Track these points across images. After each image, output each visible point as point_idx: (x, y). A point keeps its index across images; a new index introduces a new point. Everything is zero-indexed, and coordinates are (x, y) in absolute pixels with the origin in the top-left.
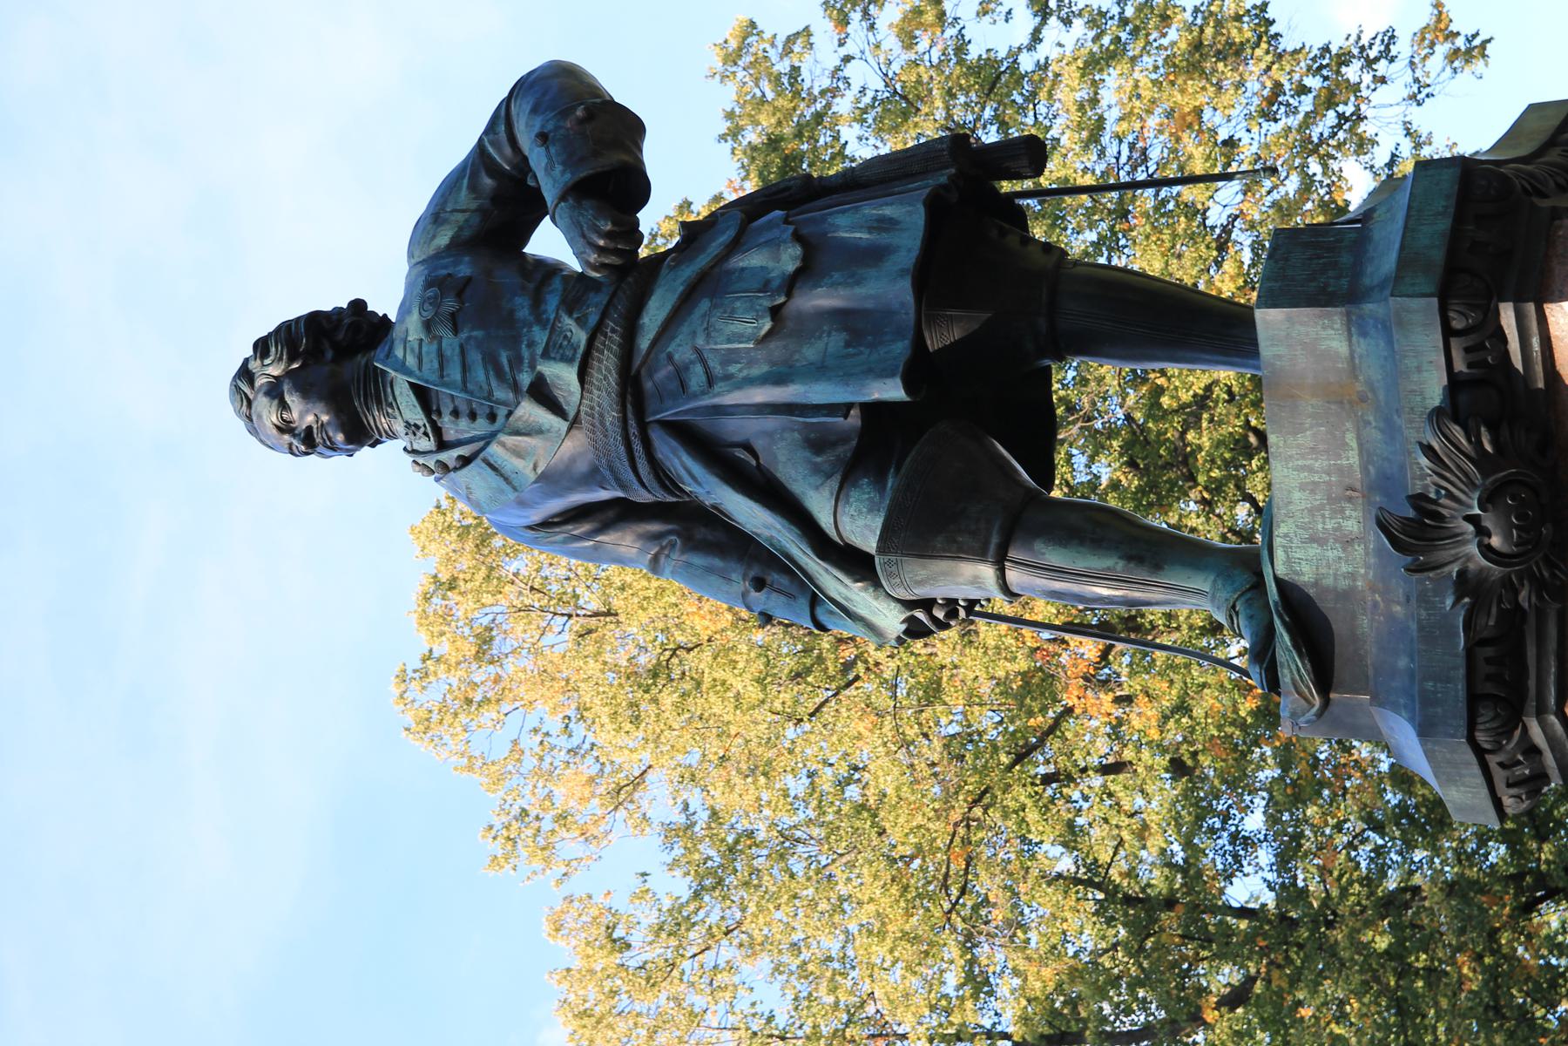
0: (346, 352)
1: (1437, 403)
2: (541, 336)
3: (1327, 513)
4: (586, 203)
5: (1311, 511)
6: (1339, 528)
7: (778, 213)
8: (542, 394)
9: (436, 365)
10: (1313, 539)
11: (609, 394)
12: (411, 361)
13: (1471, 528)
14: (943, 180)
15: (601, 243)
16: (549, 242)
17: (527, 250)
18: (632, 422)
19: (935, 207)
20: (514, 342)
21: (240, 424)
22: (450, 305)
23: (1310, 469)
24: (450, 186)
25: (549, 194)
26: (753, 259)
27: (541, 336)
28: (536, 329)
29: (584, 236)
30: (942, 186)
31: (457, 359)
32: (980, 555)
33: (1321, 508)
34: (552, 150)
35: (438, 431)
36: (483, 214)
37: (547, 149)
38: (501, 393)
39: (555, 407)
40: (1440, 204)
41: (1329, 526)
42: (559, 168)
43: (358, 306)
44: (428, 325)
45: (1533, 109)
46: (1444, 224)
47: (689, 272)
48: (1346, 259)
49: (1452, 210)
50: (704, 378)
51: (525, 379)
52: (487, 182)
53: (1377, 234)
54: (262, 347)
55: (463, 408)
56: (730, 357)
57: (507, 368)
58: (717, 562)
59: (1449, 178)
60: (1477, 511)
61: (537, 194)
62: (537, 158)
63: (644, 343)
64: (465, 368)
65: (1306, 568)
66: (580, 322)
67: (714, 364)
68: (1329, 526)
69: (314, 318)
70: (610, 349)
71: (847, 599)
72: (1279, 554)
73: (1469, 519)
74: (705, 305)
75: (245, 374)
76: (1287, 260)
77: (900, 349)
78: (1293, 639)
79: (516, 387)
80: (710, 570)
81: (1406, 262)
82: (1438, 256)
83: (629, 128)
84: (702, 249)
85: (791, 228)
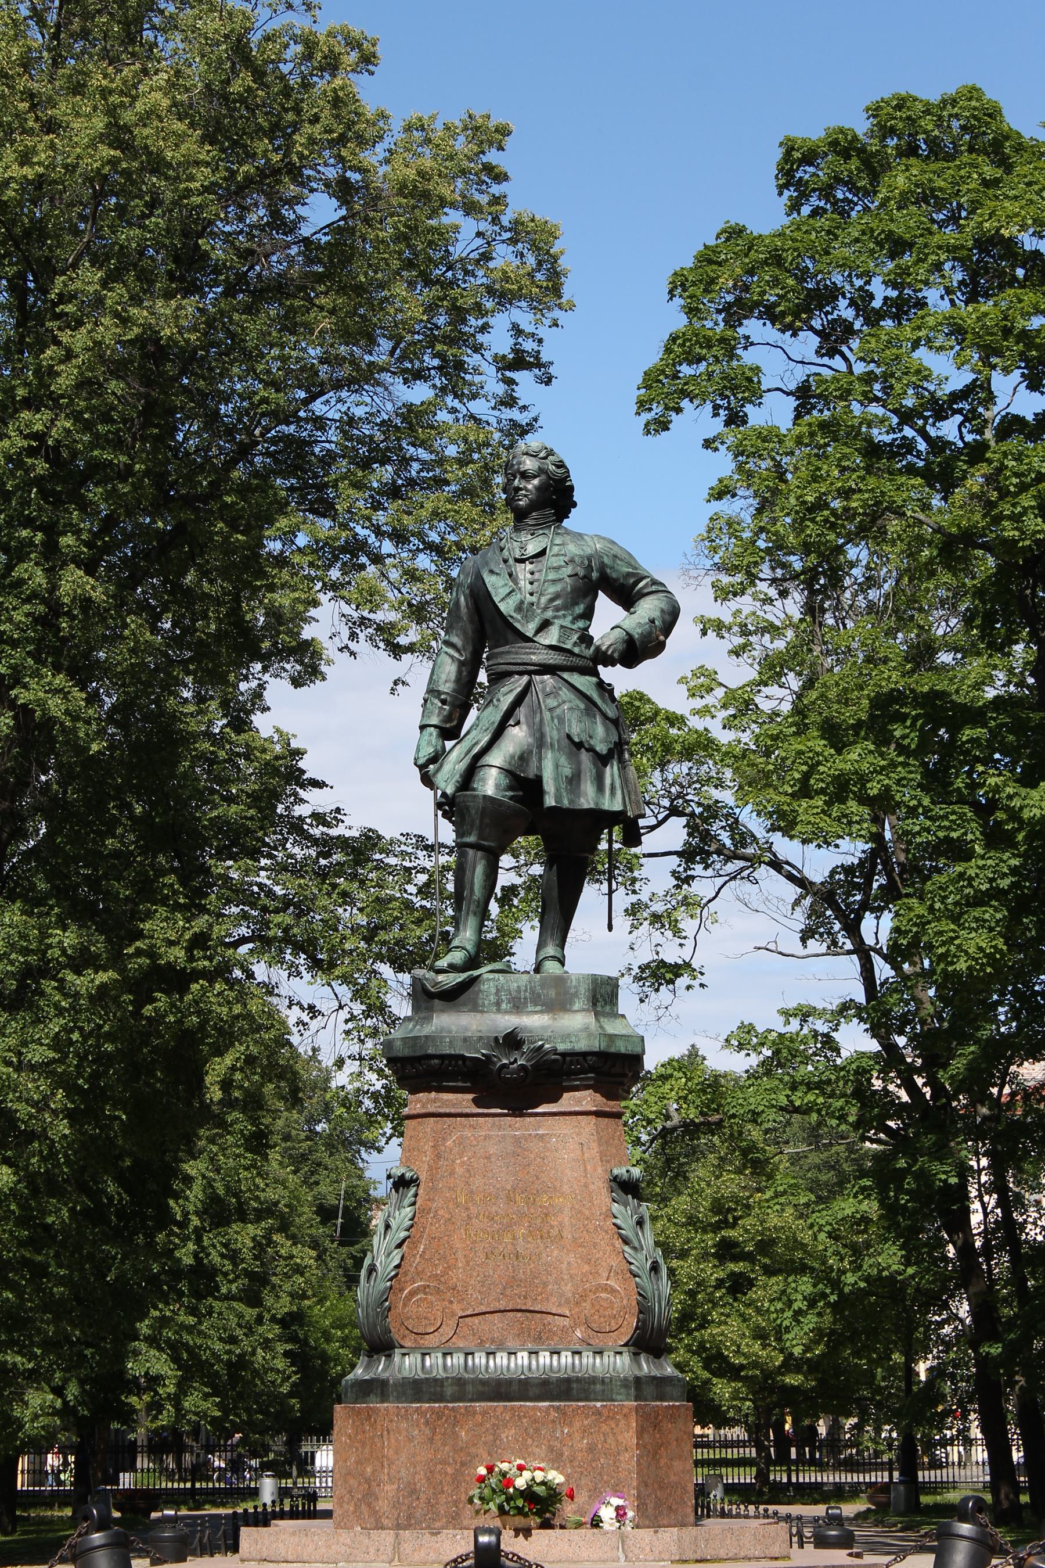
0: (553, 505)
2: (567, 622)
8: (545, 625)
12: (556, 549)
20: (565, 607)
26: (600, 730)
27: (567, 622)
32: (481, 837)
35: (521, 561)
38: (544, 600)
43: (574, 505)
44: (572, 561)
46: (623, 1050)
47: (595, 696)
48: (608, 1008)
51: (549, 614)
53: (618, 1021)
54: (561, 465)
55: (537, 576)
56: (561, 720)
63: (566, 675)
64: (554, 581)
66: (575, 644)
67: (558, 711)
69: (571, 488)
72: (491, 976)
74: (582, 706)
75: (551, 453)
77: (566, 803)
79: (545, 609)
81: (612, 1037)
82: (613, 1050)
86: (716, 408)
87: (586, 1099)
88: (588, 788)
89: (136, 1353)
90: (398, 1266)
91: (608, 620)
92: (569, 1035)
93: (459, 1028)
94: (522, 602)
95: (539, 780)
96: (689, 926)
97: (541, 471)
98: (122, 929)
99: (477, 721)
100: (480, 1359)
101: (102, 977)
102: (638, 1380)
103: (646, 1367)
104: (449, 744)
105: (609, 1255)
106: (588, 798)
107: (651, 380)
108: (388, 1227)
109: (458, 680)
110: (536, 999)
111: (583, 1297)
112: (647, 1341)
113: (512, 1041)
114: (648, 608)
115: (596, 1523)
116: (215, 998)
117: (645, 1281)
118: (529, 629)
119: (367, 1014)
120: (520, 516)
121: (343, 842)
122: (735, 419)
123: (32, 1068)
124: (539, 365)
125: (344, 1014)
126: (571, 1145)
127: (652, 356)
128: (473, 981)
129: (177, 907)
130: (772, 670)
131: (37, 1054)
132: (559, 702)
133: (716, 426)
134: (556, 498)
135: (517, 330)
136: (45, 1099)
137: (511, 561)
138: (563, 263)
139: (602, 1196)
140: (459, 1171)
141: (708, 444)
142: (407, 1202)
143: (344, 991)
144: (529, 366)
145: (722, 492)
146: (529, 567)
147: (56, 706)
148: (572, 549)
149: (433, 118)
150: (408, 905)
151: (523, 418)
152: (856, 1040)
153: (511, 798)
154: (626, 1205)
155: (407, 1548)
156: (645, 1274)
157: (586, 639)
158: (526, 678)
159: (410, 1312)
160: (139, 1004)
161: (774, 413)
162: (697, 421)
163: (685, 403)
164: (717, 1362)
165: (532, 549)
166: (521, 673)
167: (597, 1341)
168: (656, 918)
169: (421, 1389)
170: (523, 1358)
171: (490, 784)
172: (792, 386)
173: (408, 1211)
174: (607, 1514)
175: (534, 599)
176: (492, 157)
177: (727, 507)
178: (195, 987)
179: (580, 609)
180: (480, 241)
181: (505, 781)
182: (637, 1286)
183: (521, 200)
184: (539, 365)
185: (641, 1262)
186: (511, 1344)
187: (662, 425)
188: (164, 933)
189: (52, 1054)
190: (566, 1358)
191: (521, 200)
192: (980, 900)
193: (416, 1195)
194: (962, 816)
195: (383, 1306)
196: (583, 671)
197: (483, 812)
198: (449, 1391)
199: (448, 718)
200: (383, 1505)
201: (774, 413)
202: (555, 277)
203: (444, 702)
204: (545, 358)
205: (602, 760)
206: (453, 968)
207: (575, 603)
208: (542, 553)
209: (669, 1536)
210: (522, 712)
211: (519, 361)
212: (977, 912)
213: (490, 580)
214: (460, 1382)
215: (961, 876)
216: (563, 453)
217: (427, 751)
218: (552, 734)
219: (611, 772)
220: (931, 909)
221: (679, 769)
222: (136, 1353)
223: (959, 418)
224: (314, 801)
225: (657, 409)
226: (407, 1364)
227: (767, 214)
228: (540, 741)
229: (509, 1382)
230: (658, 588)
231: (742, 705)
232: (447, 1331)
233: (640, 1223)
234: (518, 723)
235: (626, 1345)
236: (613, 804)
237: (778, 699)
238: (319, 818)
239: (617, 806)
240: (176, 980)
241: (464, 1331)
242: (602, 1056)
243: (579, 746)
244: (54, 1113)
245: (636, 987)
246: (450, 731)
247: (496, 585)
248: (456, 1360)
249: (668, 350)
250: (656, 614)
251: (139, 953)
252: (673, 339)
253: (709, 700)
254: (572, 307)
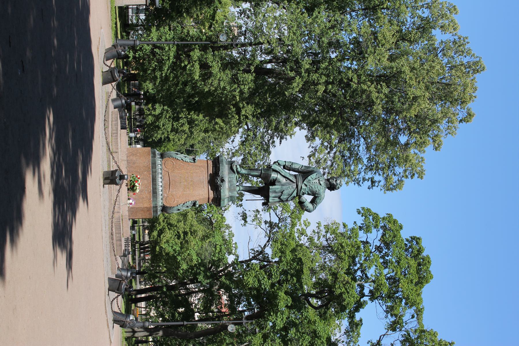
0: (331, 187)
2: (307, 190)
8: (306, 186)
24: (320, 202)
27: (307, 190)
51: (308, 186)
75: (341, 186)
77: (270, 190)
81: (224, 200)
86: (363, 224)
87: (212, 196)
88: (274, 195)
89: (160, 106)
91: (307, 198)
93: (225, 170)
95: (275, 185)
96: (255, 223)
97: (337, 184)
98: (249, 100)
99: (286, 172)
100: (160, 176)
101: (238, 98)
102: (157, 207)
103: (159, 209)
104: (282, 167)
105: (181, 201)
106: (271, 195)
107: (369, 210)
110: (231, 185)
111: (173, 196)
112: (164, 209)
113: (223, 181)
114: (310, 206)
115: (129, 199)
116: (235, 121)
117: (176, 208)
118: (305, 182)
119: (233, 153)
120: (328, 180)
121: (268, 147)
122: (361, 228)
123: (219, 83)
124: (372, 186)
125: (232, 148)
126: (203, 193)
127: (374, 210)
128: (234, 173)
129: (254, 112)
130: (311, 239)
131: (222, 84)
132: (290, 189)
133: (359, 224)
134: (332, 187)
135: (380, 182)
136: (212, 86)
138: (394, 191)
139: (193, 199)
140: (197, 171)
141: (355, 222)
143: (237, 148)
144: (372, 184)
145: (345, 226)
147: (295, 85)
148: (322, 191)
149: (424, 163)
150: (256, 161)
151: (361, 183)
152: (231, 259)
155: (123, 162)
156: (178, 208)
157: (304, 194)
159: (169, 161)
160: (233, 105)
161: (362, 236)
162: (360, 220)
163: (364, 217)
164: (161, 232)
165: (321, 182)
167: (164, 199)
168: (256, 216)
169: (154, 164)
170: (161, 184)
171: (274, 175)
172: (368, 240)
173: (189, 161)
174: (131, 201)
176: (416, 175)
177: (341, 227)
178: (237, 116)
179: (310, 192)
180: (398, 173)
181: (274, 178)
183: (407, 182)
184: (372, 186)
185: (180, 207)
186: (163, 182)
187: (359, 213)
188: (248, 110)
189: (222, 87)
190: (161, 193)
191: (407, 182)
192: (259, 281)
194: (277, 278)
195: (170, 157)
196: (297, 193)
197: (268, 174)
198: (154, 170)
199: (287, 167)
200: (131, 157)
201: (362, 236)
202: (392, 189)
204: (374, 187)
205: (279, 198)
206: (237, 169)
209: (127, 213)
210: (288, 181)
211: (373, 182)
212: (257, 281)
213: (315, 174)
214: (156, 172)
215: (264, 277)
216: (341, 188)
217: (280, 163)
218: (284, 187)
219: (277, 199)
220: (257, 271)
221: (289, 220)
222: (160, 106)
223: (361, 275)
224: (277, 140)
225: (362, 212)
226: (159, 161)
227: (405, 234)
228: (283, 185)
229: (156, 182)
230: (314, 208)
231: (302, 233)
232: (165, 169)
233: (187, 207)
236: (271, 200)
237: (304, 240)
238: (274, 142)
239: (270, 201)
240: (238, 112)
241: (166, 172)
242: (220, 199)
243: (282, 193)
244: (210, 88)
245: (241, 212)
246: (284, 167)
247: (314, 176)
248: (160, 171)
249: (375, 214)
250: (309, 208)
251: (244, 105)
252: (377, 215)
253: (303, 225)
254: (385, 193)
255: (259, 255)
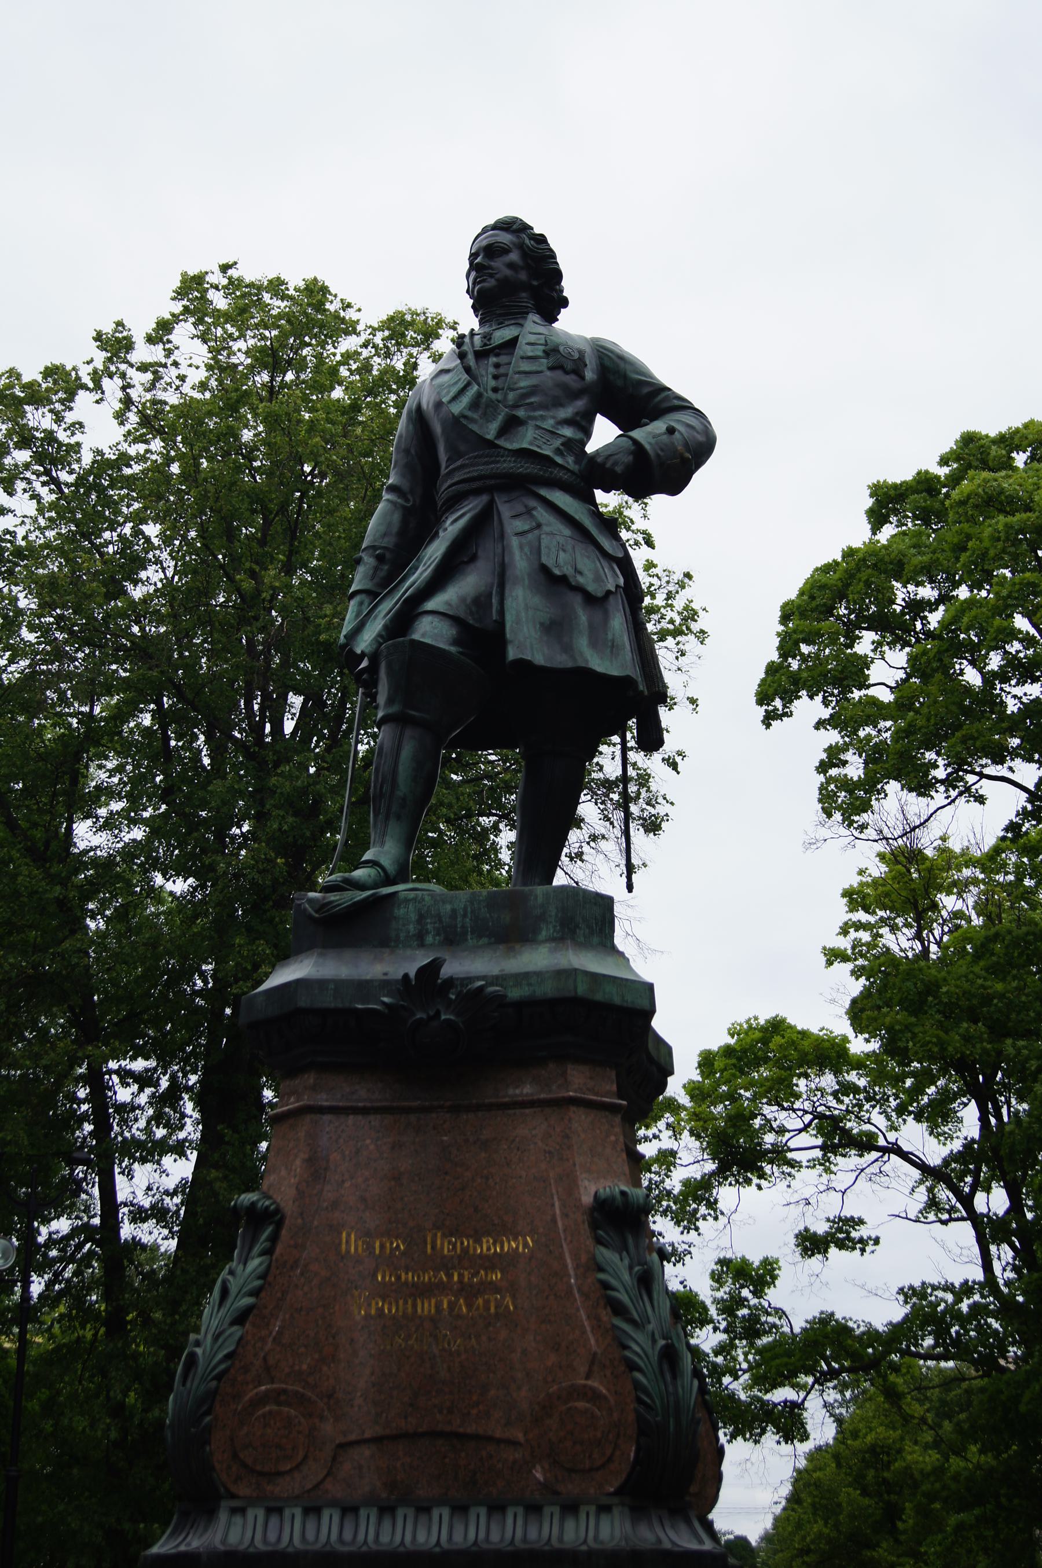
1: (510, 995)
3: (437, 925)
4: (631, 458)
5: (439, 917)
6: (428, 932)
7: (621, 581)
8: (511, 425)
9: (530, 354)
10: (421, 918)
11: (512, 468)
13: (432, 1013)
14: (641, 688)
15: (608, 465)
16: (604, 433)
17: (599, 418)
18: (493, 482)
19: (626, 682)
21: (491, 221)
22: (569, 366)
23: (465, 916)
25: (637, 434)
28: (551, 422)
29: (611, 455)
30: (637, 687)
31: (534, 368)
33: (441, 921)
34: (665, 437)
36: (622, 388)
37: (665, 434)
38: (511, 396)
39: (502, 432)
40: (629, 998)
41: (429, 926)
42: (653, 441)
43: (564, 303)
45: (669, 1049)
46: (617, 1000)
47: (588, 522)
48: (595, 940)
49: (625, 1004)
50: (521, 530)
52: (646, 390)
53: (610, 960)
54: (542, 239)
55: (502, 370)
57: (528, 401)
58: (395, 529)
59: (645, 1004)
60: (443, 1017)
61: (638, 425)
62: (659, 426)
63: (543, 492)
65: (402, 911)
68: (429, 926)
69: (558, 275)
70: (540, 470)
71: (376, 617)
72: (412, 895)
73: (438, 1014)
74: (567, 532)
76: (595, 904)
77: (539, 658)
78: (358, 902)
79: (516, 406)
80: (389, 525)
81: (596, 978)
82: (599, 997)
83: (675, 484)
84: (601, 532)
85: (613, 590)
90: (229, 1356)
92: (527, 975)
94: (479, 395)
108: (225, 1292)
109: (402, 532)
118: (491, 430)
137: (471, 357)
142: (256, 1249)
146: (493, 360)
153: (459, 652)
154: (622, 1248)
158: (484, 498)
166: (477, 492)
175: (499, 396)
182: (637, 1385)
193: (274, 1239)
203: (380, 559)
207: (558, 404)
208: (513, 343)
218: (520, 563)
234: (473, 558)
235: (618, 1492)
255: (948, 1185)
